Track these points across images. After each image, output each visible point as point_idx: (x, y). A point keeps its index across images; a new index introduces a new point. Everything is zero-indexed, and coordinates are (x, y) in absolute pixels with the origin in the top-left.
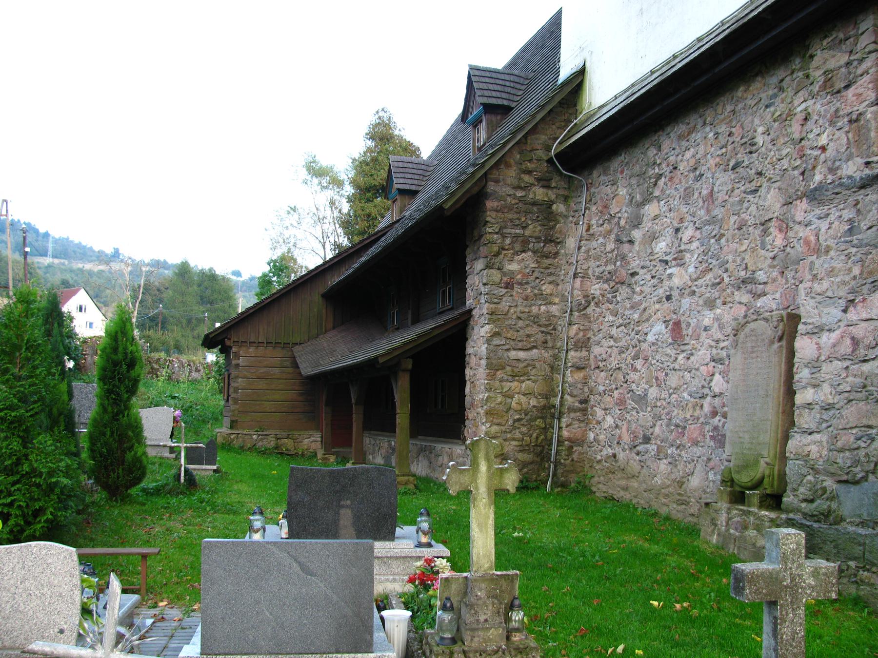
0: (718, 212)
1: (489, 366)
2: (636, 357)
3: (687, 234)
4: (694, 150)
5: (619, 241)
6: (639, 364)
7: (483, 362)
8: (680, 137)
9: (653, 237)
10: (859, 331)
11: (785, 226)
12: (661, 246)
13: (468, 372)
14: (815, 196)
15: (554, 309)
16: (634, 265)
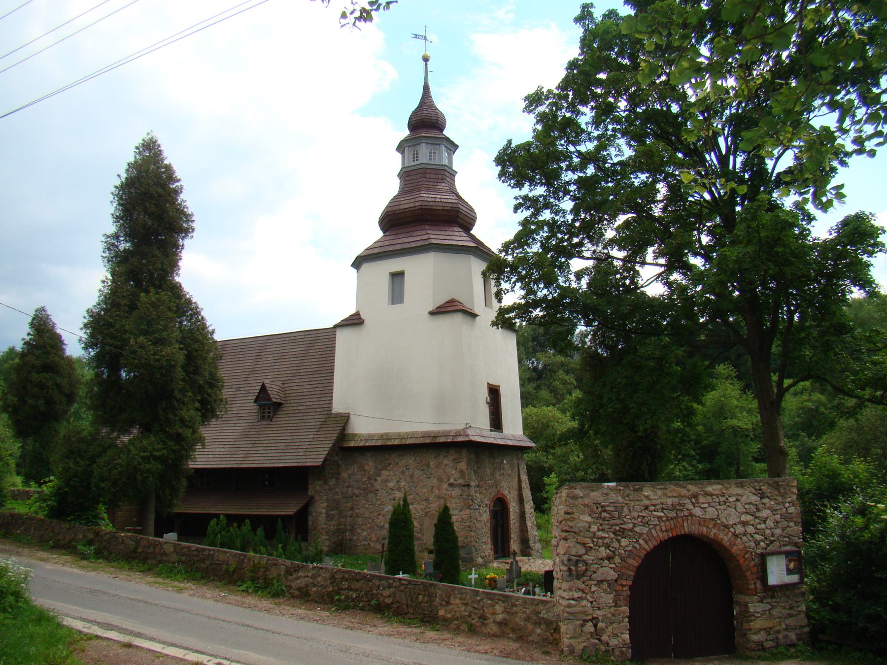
0: (416, 480)
1: (327, 517)
2: (379, 515)
3: (403, 483)
4: (410, 461)
5: (369, 478)
6: (380, 517)
7: (324, 515)
8: (400, 456)
9: (387, 481)
10: (464, 516)
11: (439, 489)
12: (391, 485)
13: (310, 518)
15: (339, 497)
16: (378, 487)
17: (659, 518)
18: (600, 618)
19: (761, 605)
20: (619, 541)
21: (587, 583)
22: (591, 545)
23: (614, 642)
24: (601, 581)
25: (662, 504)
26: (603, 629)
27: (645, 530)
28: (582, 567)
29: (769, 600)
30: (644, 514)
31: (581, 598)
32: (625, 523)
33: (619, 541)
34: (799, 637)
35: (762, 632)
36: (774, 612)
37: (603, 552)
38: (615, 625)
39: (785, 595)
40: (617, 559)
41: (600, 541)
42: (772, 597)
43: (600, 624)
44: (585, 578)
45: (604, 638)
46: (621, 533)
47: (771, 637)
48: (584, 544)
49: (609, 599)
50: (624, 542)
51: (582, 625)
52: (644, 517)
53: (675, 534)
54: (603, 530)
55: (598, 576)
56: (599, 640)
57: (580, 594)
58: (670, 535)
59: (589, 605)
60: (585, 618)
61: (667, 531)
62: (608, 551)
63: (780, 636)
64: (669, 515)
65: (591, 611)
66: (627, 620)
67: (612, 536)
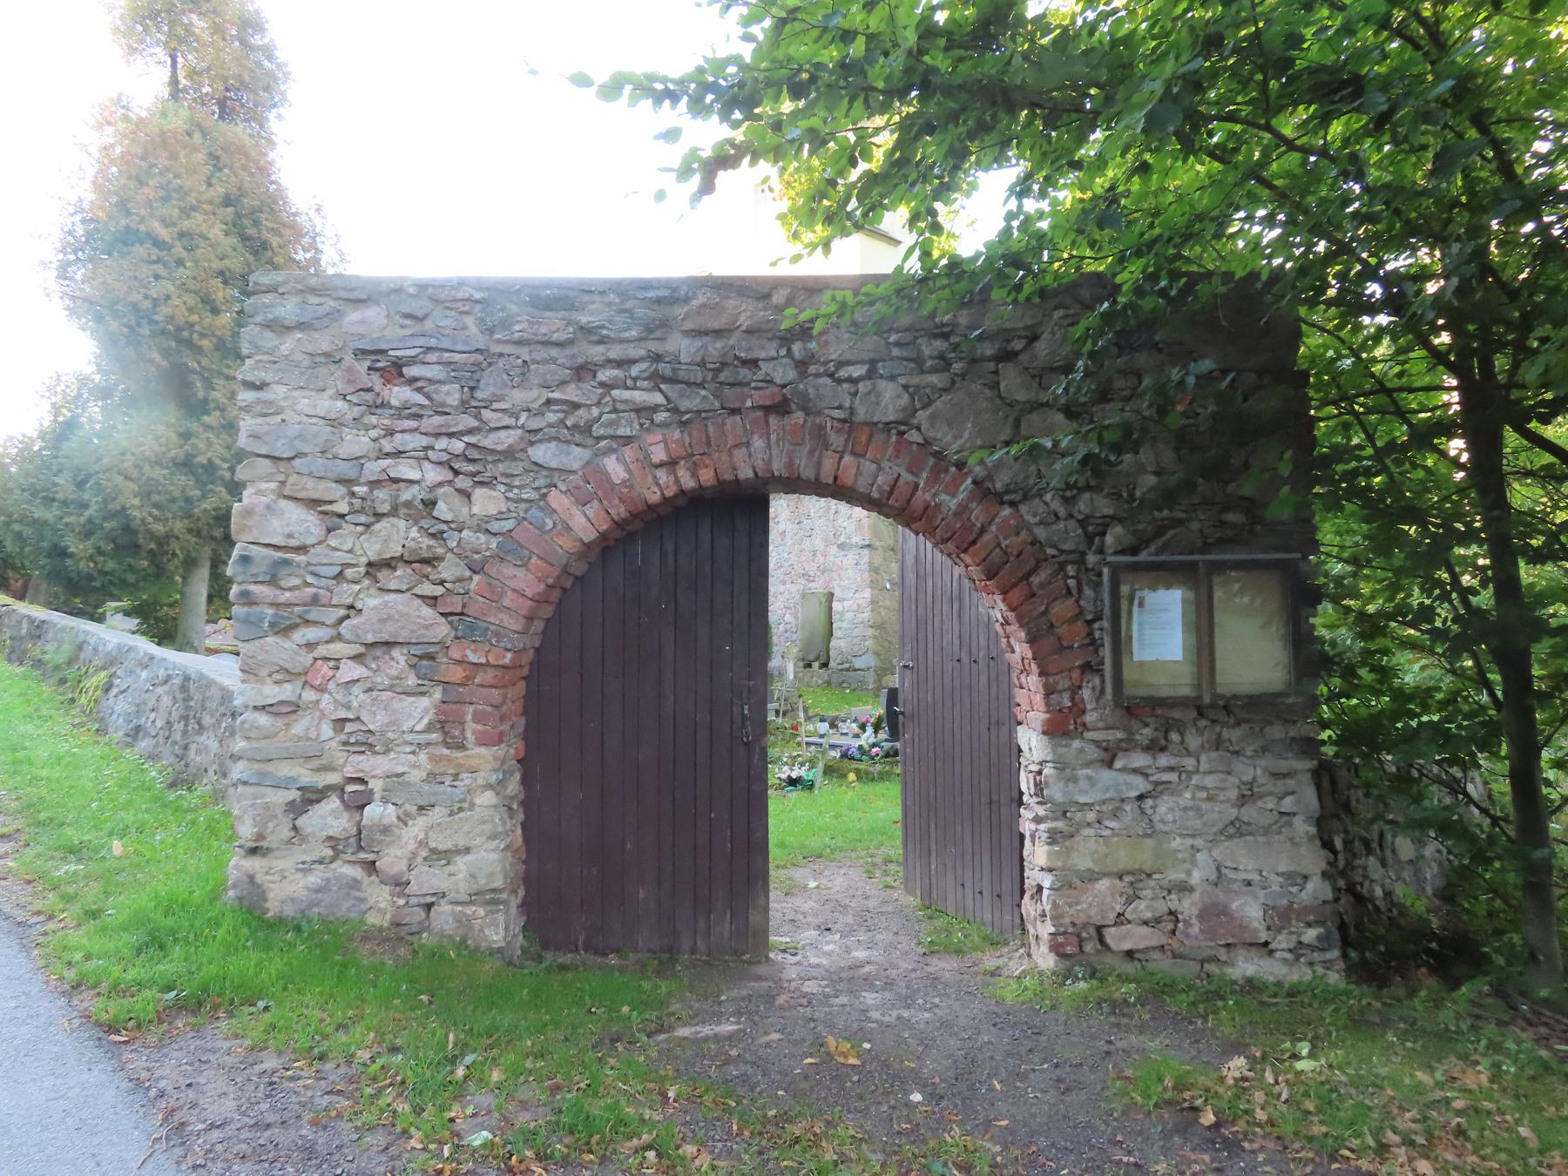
14: (841, 546)
17: (639, 410)
18: (376, 785)
19: (1105, 775)
20: (466, 495)
21: (321, 651)
22: (342, 507)
23: (427, 880)
24: (389, 644)
25: (657, 358)
26: (386, 830)
27: (577, 457)
28: (293, 589)
29: (1140, 760)
30: (571, 393)
31: (292, 708)
32: (483, 428)
33: (466, 495)
34: (1281, 917)
35: (1103, 884)
36: (1164, 808)
37: (397, 535)
38: (438, 814)
39: (1218, 745)
40: (450, 569)
41: (381, 494)
42: (1154, 748)
43: (373, 811)
44: (312, 634)
45: (392, 860)
46: (473, 468)
47: (1142, 909)
48: (312, 503)
49: (418, 711)
50: (486, 502)
51: (297, 809)
52: (576, 406)
53: (707, 477)
54: (399, 454)
55: (364, 627)
56: (371, 866)
57: (288, 691)
58: (688, 483)
59: (327, 730)
60: (307, 778)
61: (671, 464)
62: (414, 533)
63: (1188, 907)
64: (685, 404)
65: (340, 757)
66: (487, 798)
67: (433, 475)
